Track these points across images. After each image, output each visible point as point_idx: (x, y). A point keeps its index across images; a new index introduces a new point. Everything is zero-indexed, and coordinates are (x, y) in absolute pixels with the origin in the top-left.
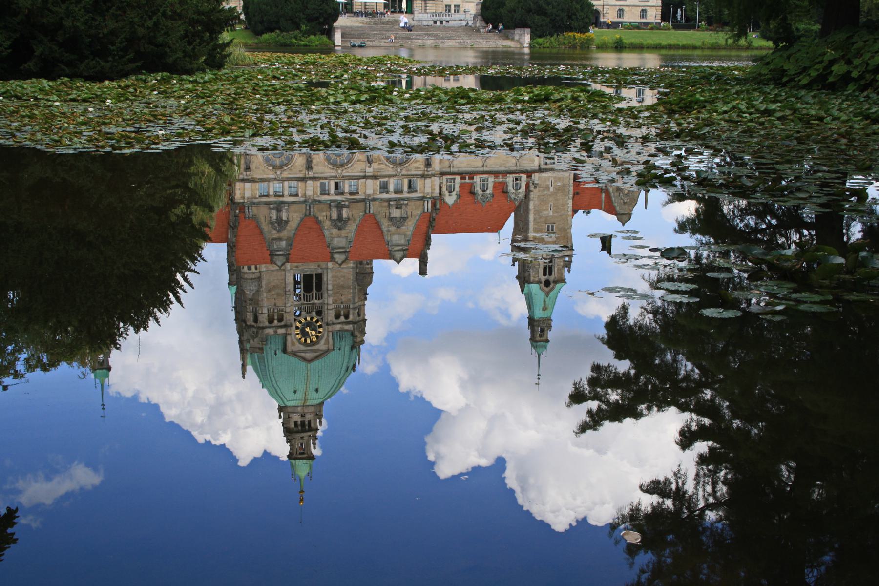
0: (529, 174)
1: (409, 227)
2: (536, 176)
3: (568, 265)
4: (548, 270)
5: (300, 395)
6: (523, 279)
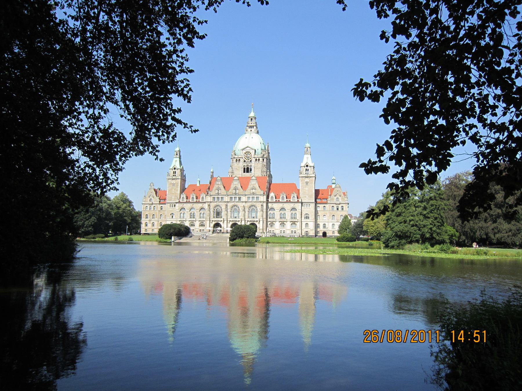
0: (179, 202)
1: (216, 187)
2: (178, 201)
4: (174, 173)
5: (251, 136)
6: (182, 170)
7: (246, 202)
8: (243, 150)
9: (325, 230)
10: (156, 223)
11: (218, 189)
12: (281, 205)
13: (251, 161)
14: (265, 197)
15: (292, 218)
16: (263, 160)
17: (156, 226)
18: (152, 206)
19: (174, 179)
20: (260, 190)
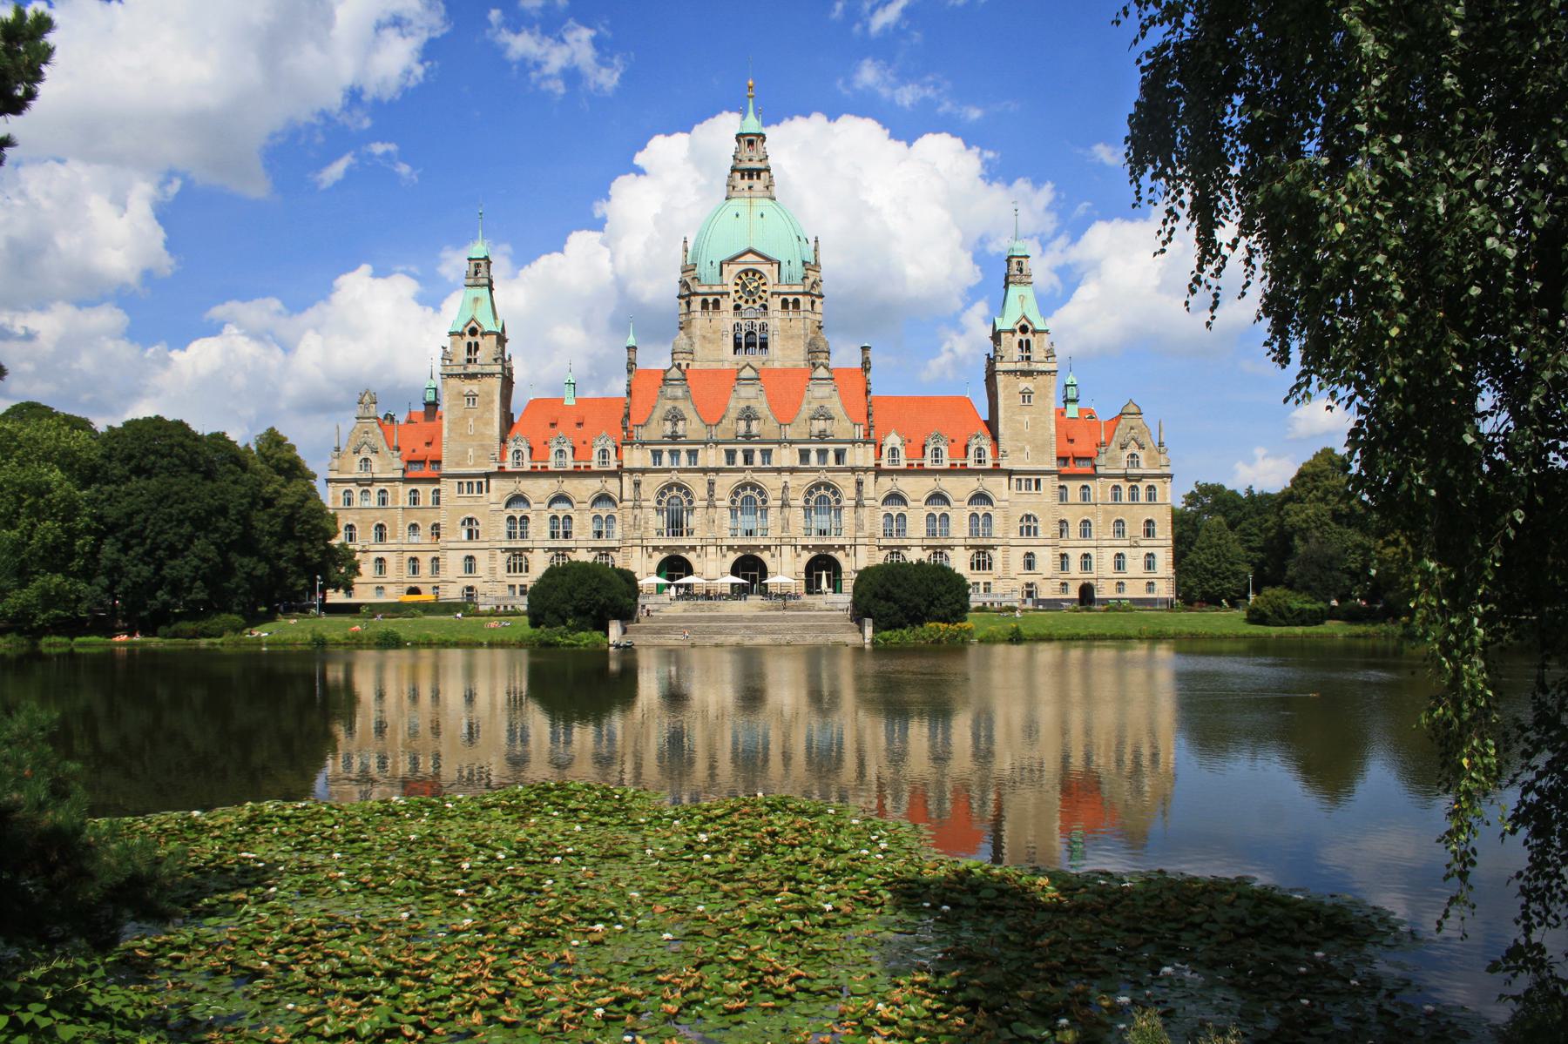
0: (502, 473)
2: (494, 468)
3: (447, 356)
4: (472, 348)
7: (792, 470)
8: (732, 260)
9: (1087, 577)
10: (391, 560)
11: (675, 417)
12: (927, 485)
13: (765, 307)
14: (871, 449)
15: (974, 533)
16: (813, 303)
17: (391, 572)
18: (374, 490)
19: (473, 376)
20: (849, 424)
